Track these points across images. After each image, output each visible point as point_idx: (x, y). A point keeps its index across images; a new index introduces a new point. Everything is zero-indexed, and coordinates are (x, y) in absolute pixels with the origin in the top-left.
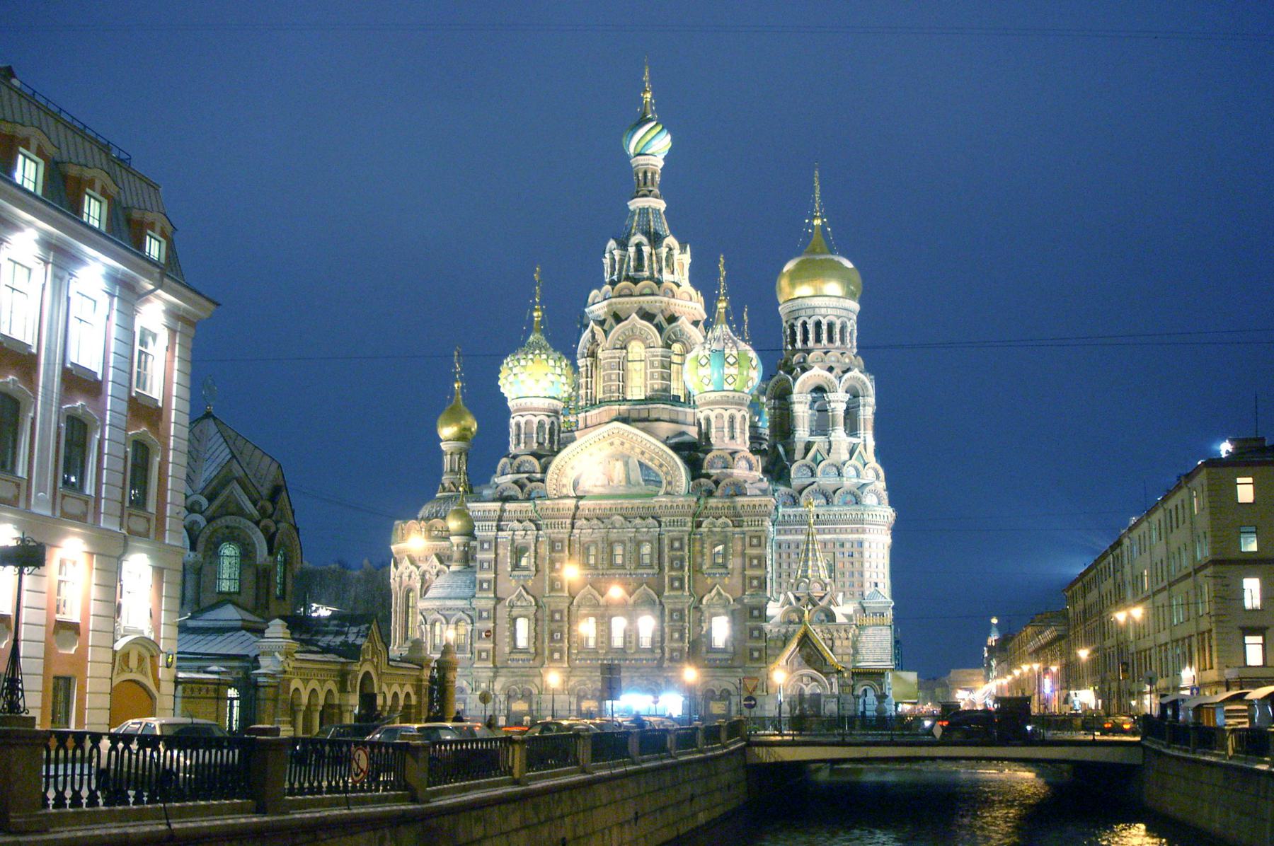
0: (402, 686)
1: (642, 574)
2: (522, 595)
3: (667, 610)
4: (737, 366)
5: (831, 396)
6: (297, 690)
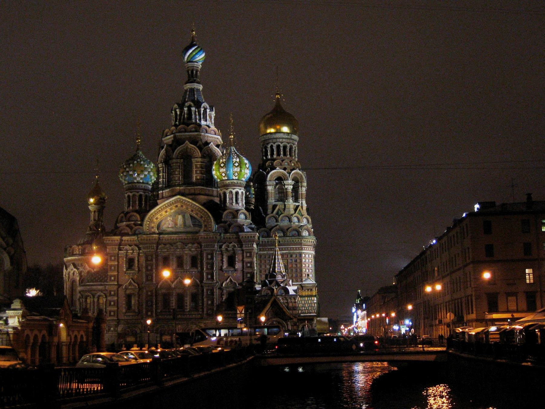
0: (79, 332)
1: (192, 272)
2: (132, 283)
3: (205, 290)
4: (239, 167)
5: (285, 182)
6: (28, 335)
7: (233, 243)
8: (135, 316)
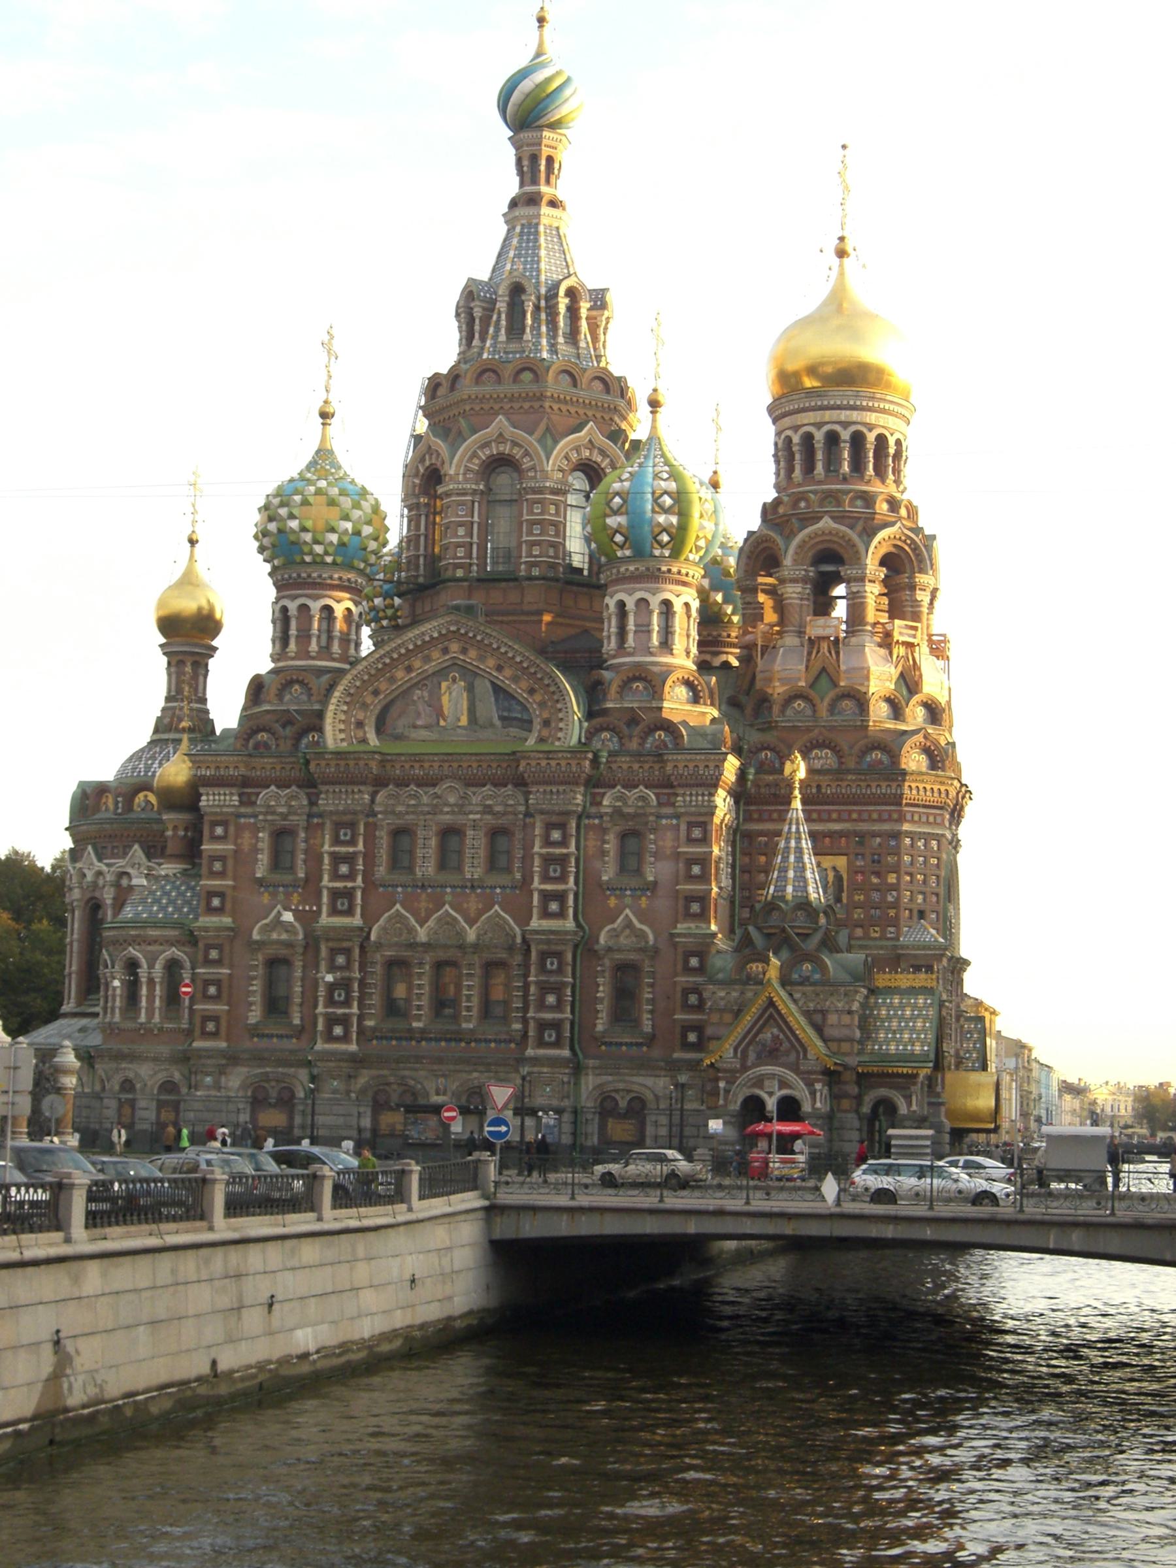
1: (493, 887)
7: (641, 787)
8: (288, 1037)
